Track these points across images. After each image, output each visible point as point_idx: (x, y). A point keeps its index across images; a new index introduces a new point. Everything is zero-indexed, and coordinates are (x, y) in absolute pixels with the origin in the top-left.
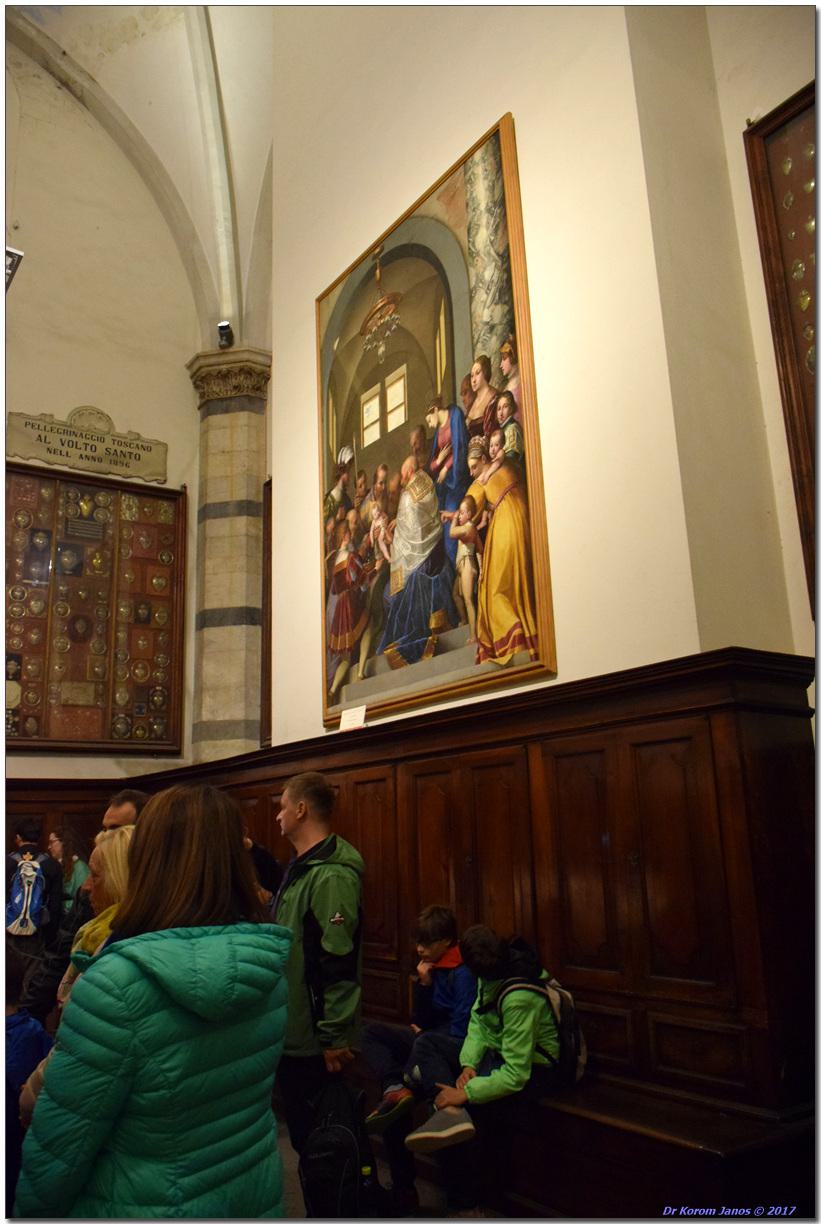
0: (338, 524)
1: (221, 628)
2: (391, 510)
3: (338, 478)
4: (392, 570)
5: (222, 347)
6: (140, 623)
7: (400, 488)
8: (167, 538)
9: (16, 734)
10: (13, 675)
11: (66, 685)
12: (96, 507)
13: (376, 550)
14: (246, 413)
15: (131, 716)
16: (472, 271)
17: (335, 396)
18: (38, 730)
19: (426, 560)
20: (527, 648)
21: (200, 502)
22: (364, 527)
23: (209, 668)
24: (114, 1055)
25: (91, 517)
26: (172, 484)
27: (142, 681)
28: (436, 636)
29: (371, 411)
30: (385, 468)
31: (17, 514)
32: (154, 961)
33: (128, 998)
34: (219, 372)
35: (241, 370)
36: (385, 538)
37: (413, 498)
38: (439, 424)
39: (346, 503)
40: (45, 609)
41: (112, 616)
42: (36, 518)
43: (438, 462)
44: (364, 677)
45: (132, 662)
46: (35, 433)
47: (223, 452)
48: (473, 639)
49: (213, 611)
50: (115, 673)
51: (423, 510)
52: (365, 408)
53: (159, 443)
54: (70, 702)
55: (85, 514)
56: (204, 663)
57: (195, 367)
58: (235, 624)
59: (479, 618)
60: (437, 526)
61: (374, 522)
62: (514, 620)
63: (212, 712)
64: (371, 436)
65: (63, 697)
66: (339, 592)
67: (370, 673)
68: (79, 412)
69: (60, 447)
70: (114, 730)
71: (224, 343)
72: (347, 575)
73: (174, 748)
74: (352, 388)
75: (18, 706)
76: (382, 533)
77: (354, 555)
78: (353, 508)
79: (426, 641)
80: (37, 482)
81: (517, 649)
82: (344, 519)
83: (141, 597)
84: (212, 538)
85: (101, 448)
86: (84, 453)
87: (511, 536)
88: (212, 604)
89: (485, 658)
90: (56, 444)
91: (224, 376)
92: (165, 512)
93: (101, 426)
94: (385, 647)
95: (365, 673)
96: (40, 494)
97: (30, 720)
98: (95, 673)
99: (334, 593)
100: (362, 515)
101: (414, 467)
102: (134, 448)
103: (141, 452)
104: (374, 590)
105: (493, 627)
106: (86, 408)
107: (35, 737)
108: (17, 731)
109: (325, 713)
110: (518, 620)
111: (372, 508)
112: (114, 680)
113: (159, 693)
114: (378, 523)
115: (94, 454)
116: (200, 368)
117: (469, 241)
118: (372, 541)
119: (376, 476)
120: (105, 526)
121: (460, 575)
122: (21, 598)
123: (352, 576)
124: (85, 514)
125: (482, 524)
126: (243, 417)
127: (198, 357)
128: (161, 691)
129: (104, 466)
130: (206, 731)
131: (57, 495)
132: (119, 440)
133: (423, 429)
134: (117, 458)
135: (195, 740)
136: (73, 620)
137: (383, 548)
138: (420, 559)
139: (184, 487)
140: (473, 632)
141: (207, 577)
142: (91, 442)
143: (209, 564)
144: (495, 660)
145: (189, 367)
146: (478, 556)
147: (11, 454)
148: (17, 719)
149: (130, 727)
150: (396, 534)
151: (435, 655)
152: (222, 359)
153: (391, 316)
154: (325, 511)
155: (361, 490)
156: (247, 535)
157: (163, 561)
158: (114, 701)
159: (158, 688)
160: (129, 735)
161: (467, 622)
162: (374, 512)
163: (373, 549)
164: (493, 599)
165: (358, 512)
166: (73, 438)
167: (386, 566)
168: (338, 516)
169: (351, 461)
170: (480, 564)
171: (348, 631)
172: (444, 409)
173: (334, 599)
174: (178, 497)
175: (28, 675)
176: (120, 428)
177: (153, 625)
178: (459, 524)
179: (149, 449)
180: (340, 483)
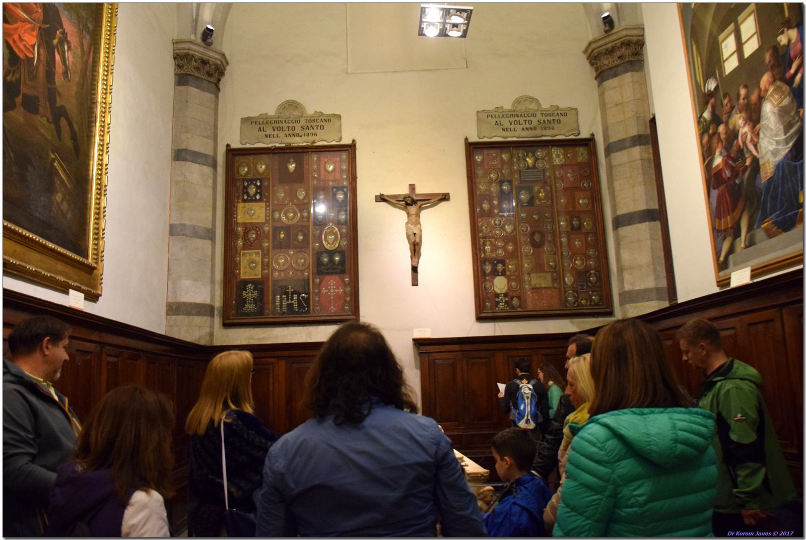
0: (711, 137)
1: (631, 226)
2: (754, 117)
3: (707, 103)
4: (761, 162)
5: (606, 32)
6: (575, 230)
7: (761, 99)
8: (585, 171)
9: (508, 308)
10: (502, 272)
11: (533, 275)
12: (536, 160)
13: (745, 151)
14: (629, 74)
15: (577, 292)
17: (697, 43)
18: (520, 305)
19: (791, 151)
21: (604, 144)
22: (733, 135)
23: (626, 255)
24: (601, 483)
25: (534, 167)
26: (584, 135)
27: (581, 268)
29: (728, 46)
30: (746, 86)
31: (490, 174)
32: (621, 427)
33: (606, 449)
34: (607, 50)
35: (623, 44)
36: (752, 140)
37: (773, 104)
38: (789, 41)
39: (716, 120)
40: (515, 229)
41: (556, 227)
42: (502, 173)
43: (792, 71)
44: (747, 247)
45: (573, 256)
46: (494, 121)
47: (617, 105)
49: (624, 216)
50: (563, 264)
51: (783, 112)
52: (723, 45)
53: (571, 109)
54: (537, 286)
55: (531, 165)
56: (622, 252)
57: (590, 51)
58: (640, 222)
60: (798, 121)
61: (741, 130)
63: (632, 284)
64: (731, 65)
65: (533, 283)
67: (751, 243)
68: (518, 101)
69: (509, 126)
70: (567, 301)
71: (607, 28)
72: (723, 174)
73: (608, 310)
74: (710, 34)
75: (506, 291)
76: (749, 137)
77: (727, 157)
79: (798, 212)
80: (499, 151)
82: (716, 133)
83: (573, 214)
84: (616, 166)
85: (535, 121)
86: (524, 126)
88: (621, 211)
90: (507, 125)
91: (610, 52)
92: (582, 154)
93: (533, 106)
94: (762, 222)
95: (747, 244)
96: (502, 158)
97: (515, 299)
98: (551, 266)
99: (714, 188)
100: (731, 127)
101: (770, 80)
102: (556, 115)
103: (561, 118)
104: (747, 182)
106: (521, 97)
107: (519, 309)
108: (508, 306)
109: (717, 277)
111: (738, 120)
112: (563, 270)
113: (593, 275)
114: (745, 130)
115: (530, 126)
116: (593, 51)
118: (741, 144)
119: (738, 95)
120: (544, 171)
122: (499, 225)
123: (728, 173)
124: (531, 165)
126: (627, 78)
127: (590, 44)
128: (594, 273)
129: (538, 132)
130: (629, 297)
131: (512, 157)
132: (545, 113)
133: (776, 48)
134: (546, 125)
135: (622, 304)
136: (532, 234)
137: (751, 148)
138: (784, 150)
139: (593, 135)
141: (616, 193)
142: (528, 119)
143: (617, 184)
145: (585, 52)
147: (482, 136)
148: (507, 299)
149: (576, 299)
150: (761, 135)
152: (607, 40)
154: (699, 130)
155: (727, 108)
156: (641, 159)
157: (584, 187)
158: (565, 283)
159: (592, 272)
160: (576, 304)
162: (740, 122)
163: (743, 150)
165: (727, 124)
166: (517, 119)
167: (755, 161)
168: (711, 131)
169: (717, 88)
171: (729, 215)
172: (793, 28)
173: (715, 193)
174: (589, 143)
175: (509, 271)
176: (545, 106)
177: (584, 231)
179: (566, 115)
180: (709, 107)
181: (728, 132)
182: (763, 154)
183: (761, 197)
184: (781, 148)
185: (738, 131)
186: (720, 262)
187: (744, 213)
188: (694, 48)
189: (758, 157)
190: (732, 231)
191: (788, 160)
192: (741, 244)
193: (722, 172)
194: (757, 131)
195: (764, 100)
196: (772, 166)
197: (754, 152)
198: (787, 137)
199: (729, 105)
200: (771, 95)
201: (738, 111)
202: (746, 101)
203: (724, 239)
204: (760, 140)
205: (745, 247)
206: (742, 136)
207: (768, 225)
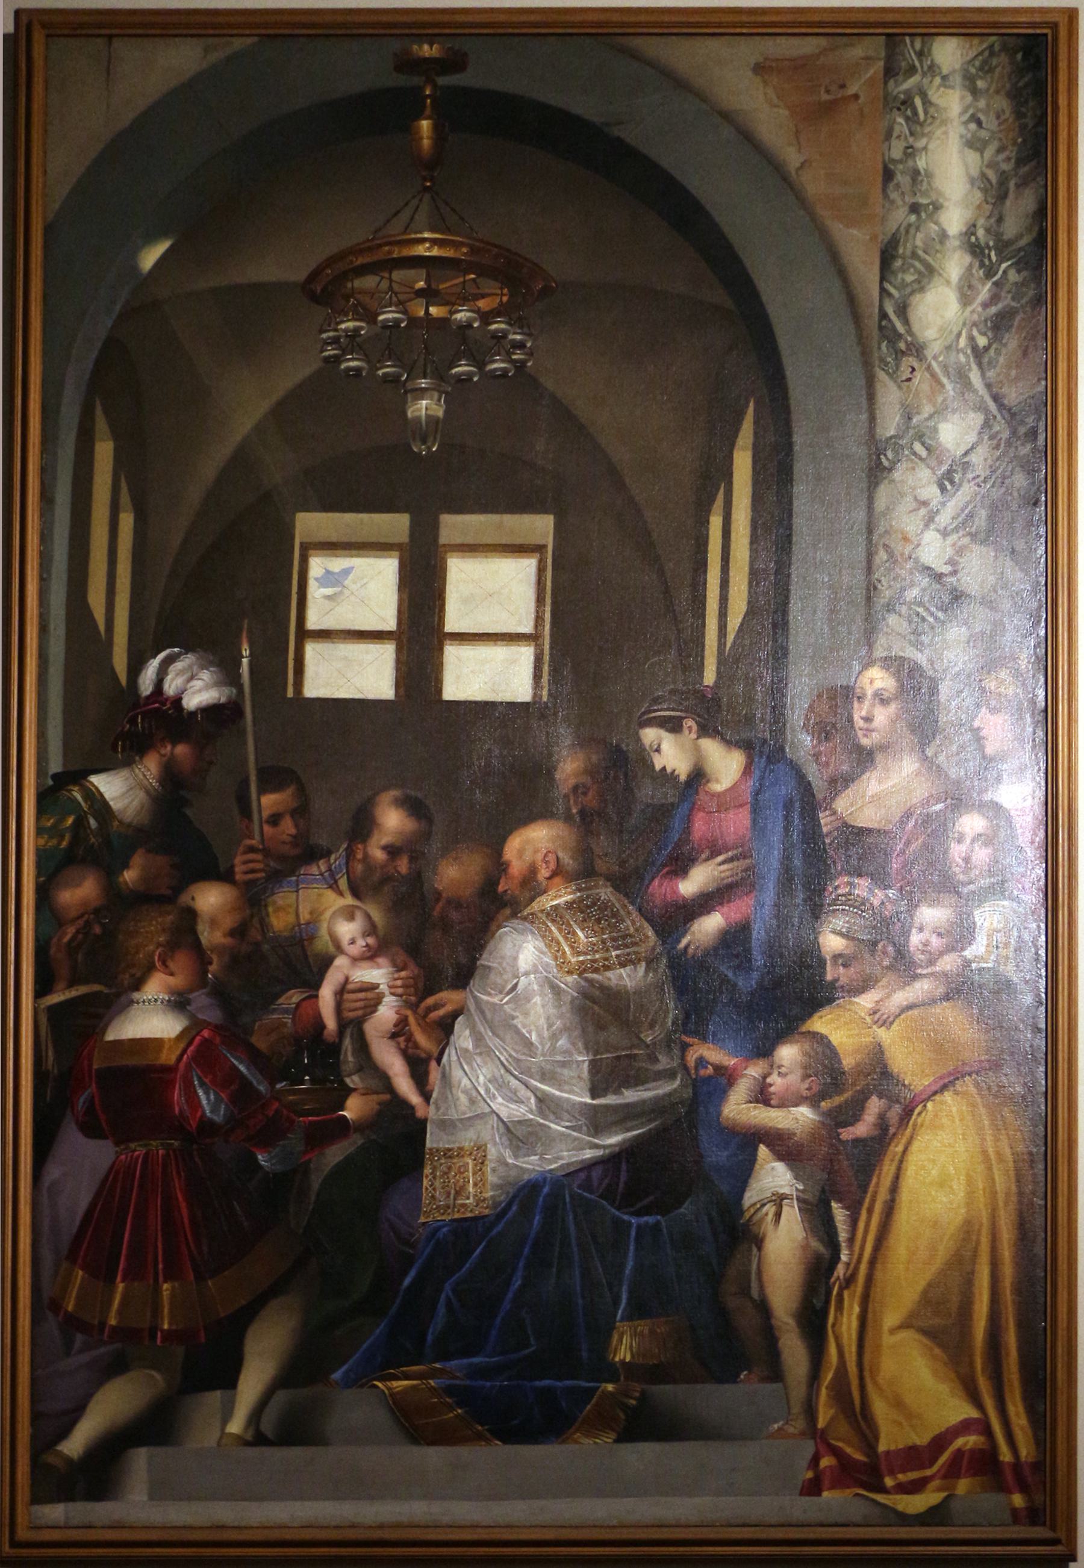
16: (889, 396)
19: (612, 1161)
20: (1003, 1488)
28: (637, 1388)
30: (414, 807)
36: (399, 1032)
43: (690, 886)
48: (798, 1425)
52: (317, 565)
59: (829, 1376)
60: (671, 1075)
61: (340, 962)
62: (961, 1411)
66: (122, 1137)
76: (387, 1012)
78: (226, 877)
79: (592, 1391)
81: (963, 1486)
87: (970, 1194)
89: (837, 1484)
95: (267, 1426)
99: (91, 1130)
100: (279, 922)
105: (880, 1408)
110: (974, 1414)
117: (883, 291)
118: (331, 1023)
121: (759, 1242)
125: (862, 1129)
140: (796, 1409)
144: (880, 1498)
146: (839, 1213)
150: (463, 1037)
151: (617, 1441)
153: (486, 317)
161: (775, 1373)
162: (347, 930)
163: (335, 1049)
164: (887, 1340)
168: (129, 876)
170: (843, 1235)
178: (762, 1096)
180: (150, 768)
181: (255, 934)
182: (454, 1115)
183: (405, 1273)
184: (562, 1134)
185: (327, 962)
186: (51, 1459)
187: (274, 1304)
188: (104, 451)
189: (420, 1113)
190: (180, 1351)
191: (587, 1186)
192: (226, 1418)
193: (171, 1083)
194: (441, 1012)
195: (514, 915)
196: (491, 1178)
197: (405, 1086)
198: (594, 1106)
199: (288, 827)
200: (555, 914)
201: (343, 883)
202: (403, 865)
203: (116, 1367)
204: (450, 1055)
205: (249, 1437)
206: (341, 992)
207: (414, 1388)
